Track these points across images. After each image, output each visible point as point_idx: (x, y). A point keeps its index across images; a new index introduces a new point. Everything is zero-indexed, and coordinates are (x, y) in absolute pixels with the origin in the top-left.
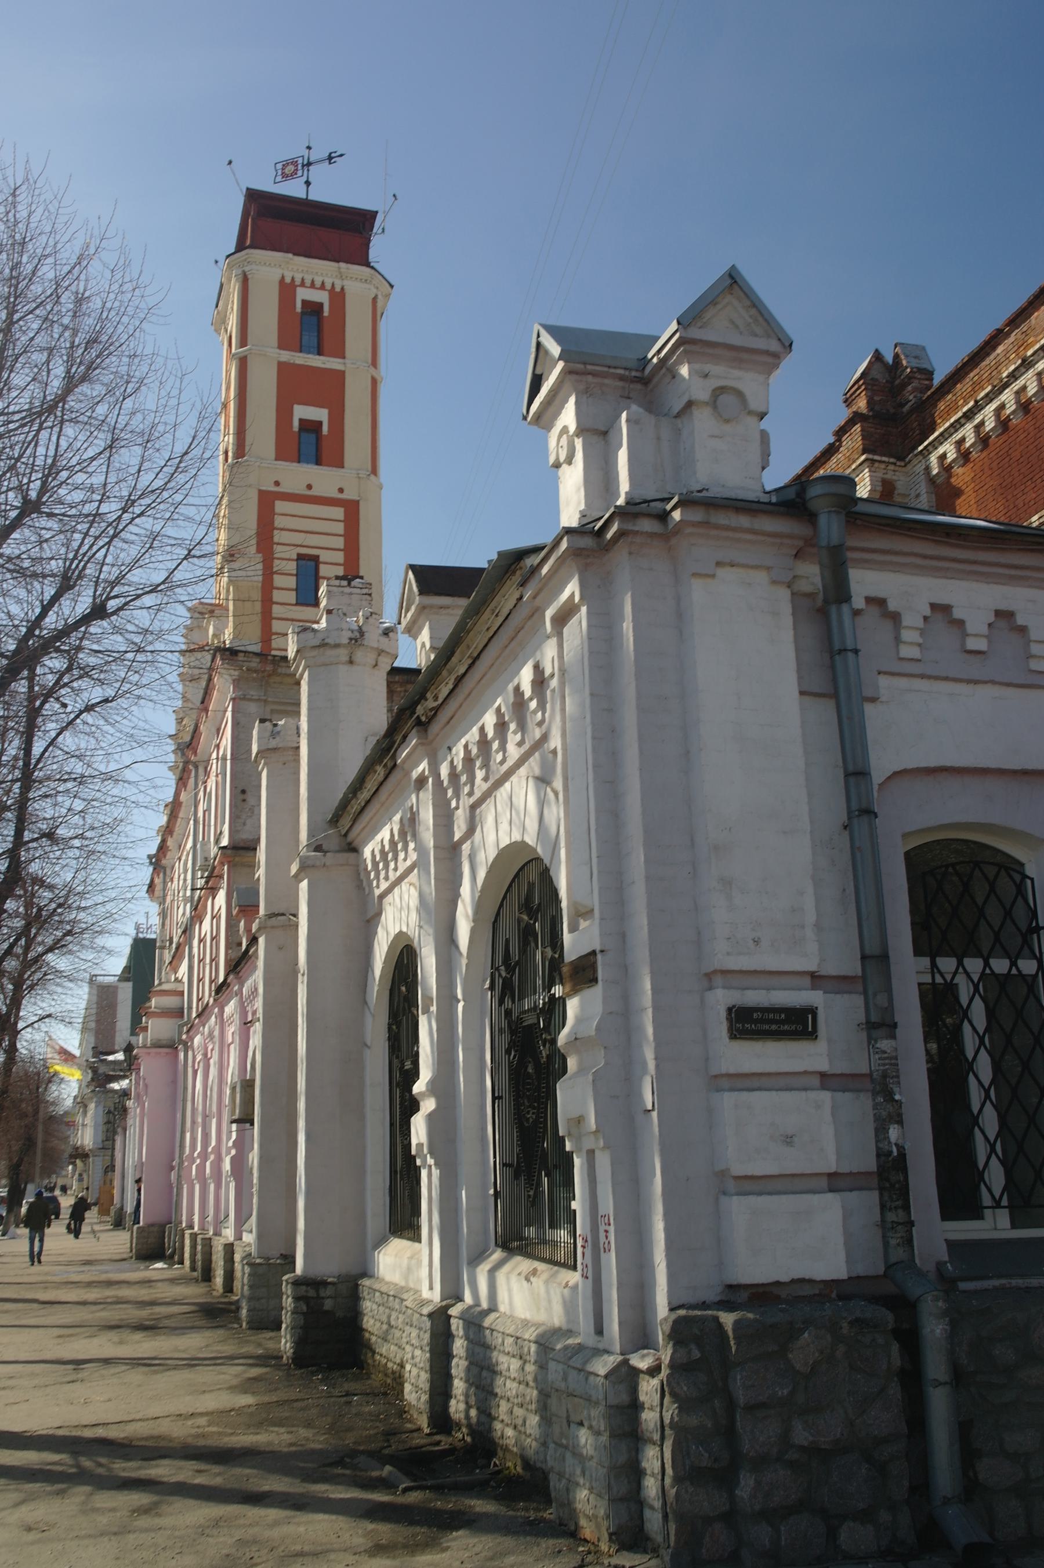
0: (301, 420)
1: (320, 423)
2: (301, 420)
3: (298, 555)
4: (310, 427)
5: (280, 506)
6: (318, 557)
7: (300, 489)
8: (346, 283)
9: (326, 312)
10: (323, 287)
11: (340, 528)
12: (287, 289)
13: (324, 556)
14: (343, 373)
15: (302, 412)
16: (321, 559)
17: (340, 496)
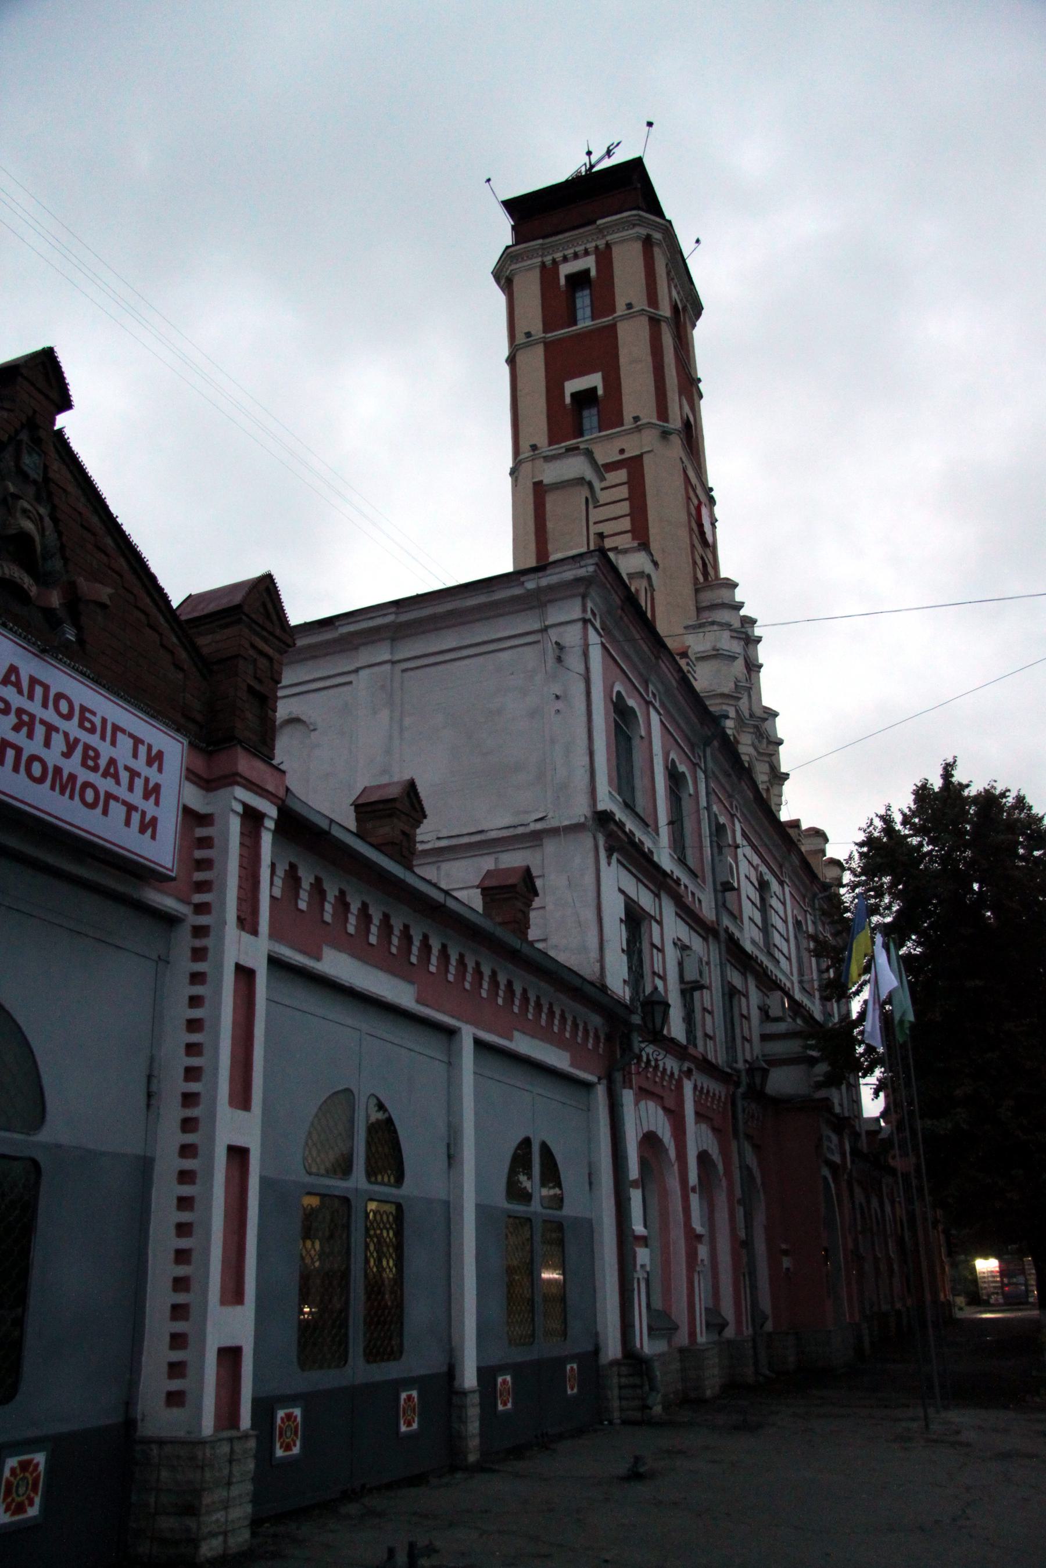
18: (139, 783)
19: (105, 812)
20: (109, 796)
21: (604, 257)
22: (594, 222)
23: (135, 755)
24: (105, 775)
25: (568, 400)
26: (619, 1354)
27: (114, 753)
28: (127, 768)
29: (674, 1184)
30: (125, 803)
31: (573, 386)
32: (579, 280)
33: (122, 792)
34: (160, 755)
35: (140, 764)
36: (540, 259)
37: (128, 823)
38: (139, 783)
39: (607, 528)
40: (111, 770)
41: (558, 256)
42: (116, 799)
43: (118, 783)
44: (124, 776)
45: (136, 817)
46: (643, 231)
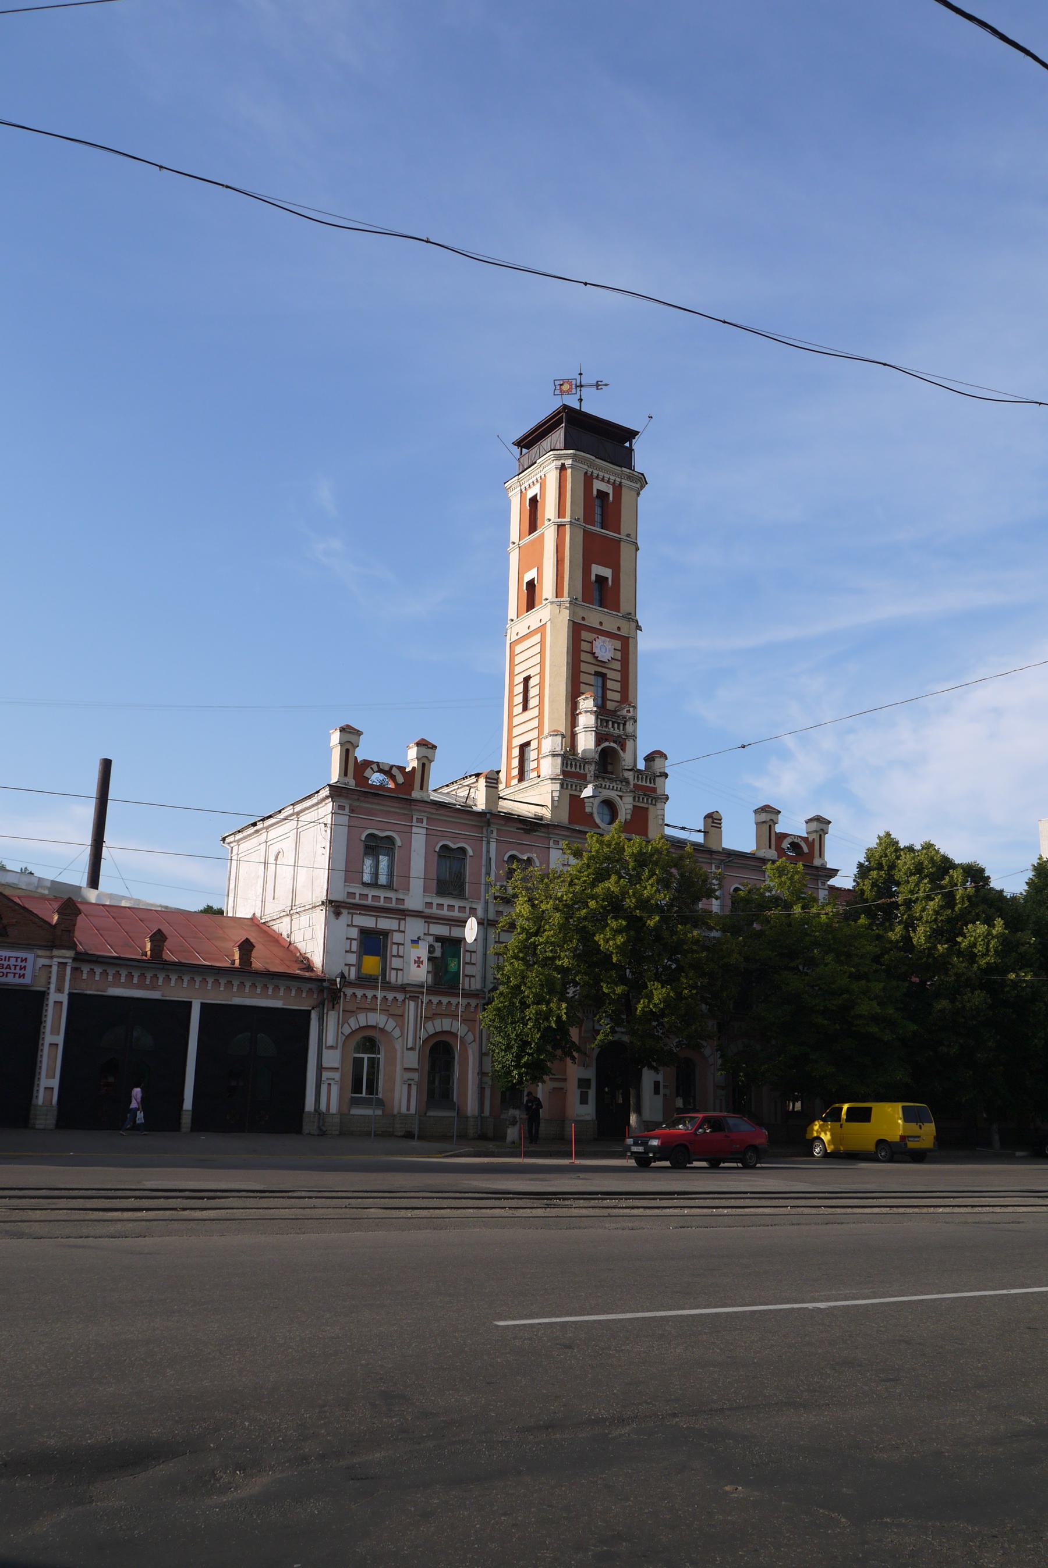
0: (596, 575)
1: (607, 578)
2: (596, 575)
3: (595, 672)
4: (601, 580)
5: (585, 635)
6: (606, 674)
8: (623, 481)
9: (611, 498)
10: (608, 482)
12: (588, 479)
13: (610, 674)
15: (597, 570)
16: (608, 676)
18: (18, 968)
19: (7, 976)
20: (7, 973)
22: (535, 463)
23: (17, 961)
24: (6, 968)
26: (312, 1109)
27: (9, 963)
28: (13, 965)
29: (398, 1046)
30: (13, 973)
31: (528, 577)
33: (13, 971)
34: (26, 959)
35: (19, 963)
36: (519, 488)
37: (14, 977)
38: (18, 968)
40: (9, 967)
41: (527, 484)
42: (10, 973)
43: (10, 969)
44: (12, 968)
45: (17, 976)
46: (559, 463)
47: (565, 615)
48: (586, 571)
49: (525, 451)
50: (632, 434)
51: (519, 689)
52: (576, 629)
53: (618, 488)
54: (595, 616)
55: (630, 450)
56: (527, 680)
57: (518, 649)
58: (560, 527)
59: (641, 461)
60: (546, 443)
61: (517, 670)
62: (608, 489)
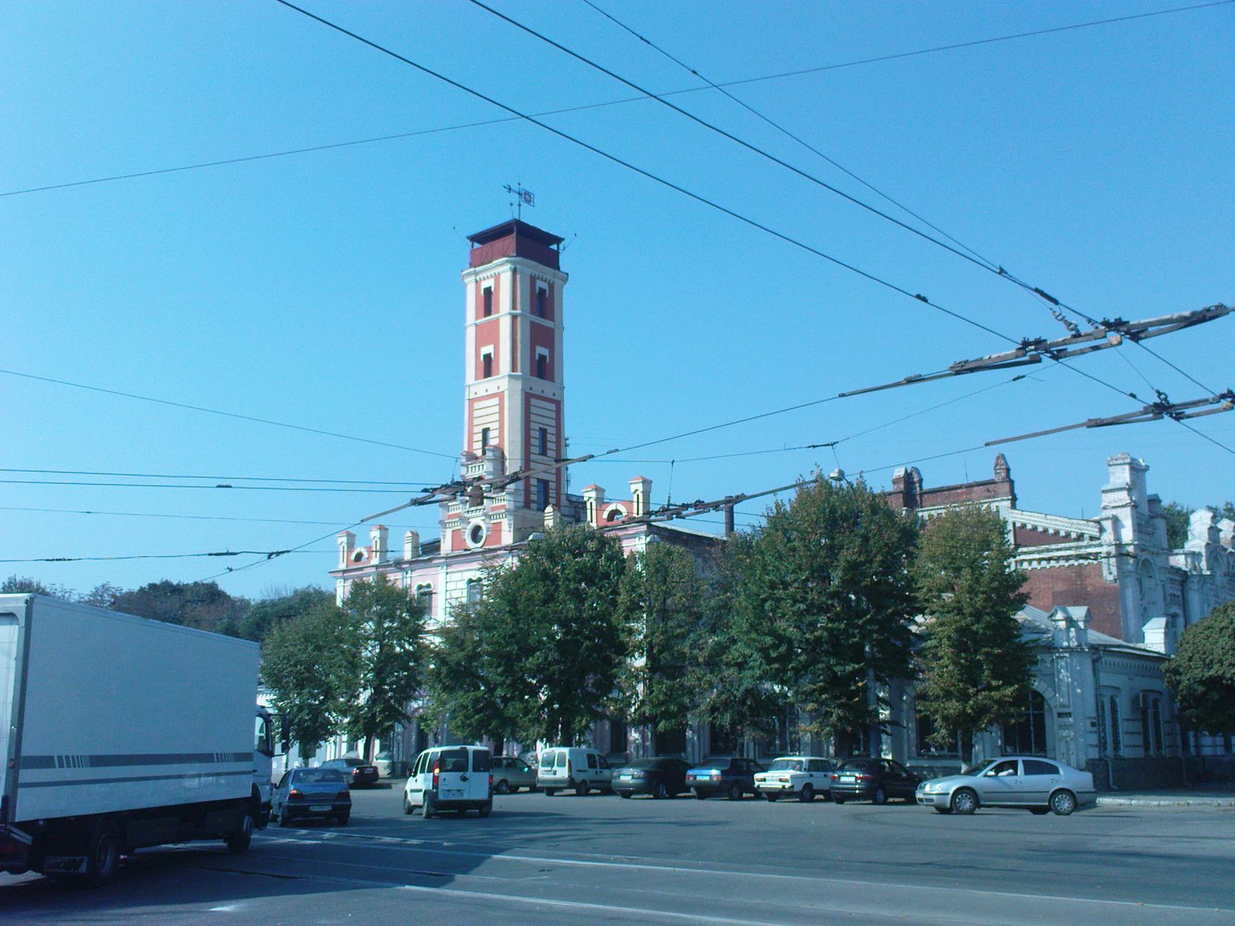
0: (540, 355)
2: (540, 355)
4: (542, 358)
5: (534, 401)
6: (546, 430)
7: (539, 393)
10: (546, 281)
11: (553, 415)
12: (533, 279)
13: (551, 430)
14: (553, 330)
15: (541, 351)
17: (553, 397)
21: (497, 278)
25: (482, 358)
31: (486, 350)
32: (488, 291)
39: (492, 426)
47: (519, 385)
48: (533, 351)
49: (477, 245)
50: (558, 240)
51: (480, 437)
52: (528, 397)
53: (551, 286)
54: (540, 385)
55: (556, 254)
56: (485, 432)
57: (477, 405)
58: (514, 317)
59: (566, 261)
60: (499, 244)
61: (476, 422)
62: (545, 286)
